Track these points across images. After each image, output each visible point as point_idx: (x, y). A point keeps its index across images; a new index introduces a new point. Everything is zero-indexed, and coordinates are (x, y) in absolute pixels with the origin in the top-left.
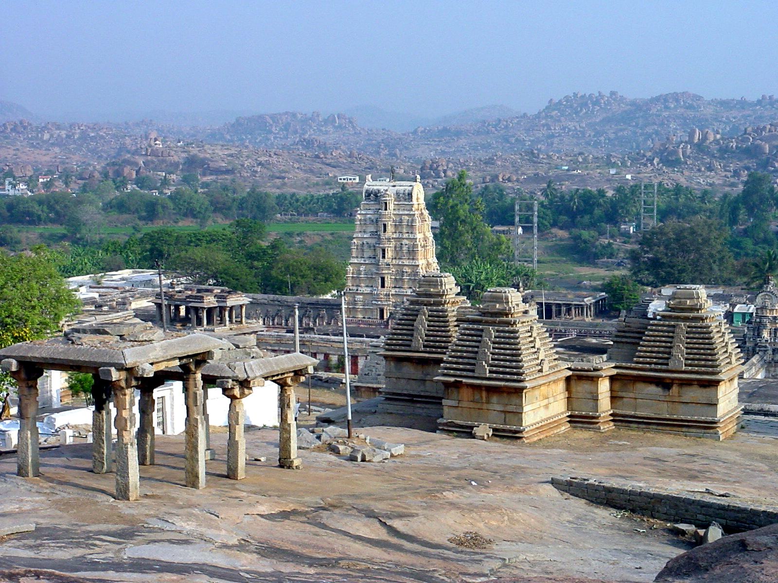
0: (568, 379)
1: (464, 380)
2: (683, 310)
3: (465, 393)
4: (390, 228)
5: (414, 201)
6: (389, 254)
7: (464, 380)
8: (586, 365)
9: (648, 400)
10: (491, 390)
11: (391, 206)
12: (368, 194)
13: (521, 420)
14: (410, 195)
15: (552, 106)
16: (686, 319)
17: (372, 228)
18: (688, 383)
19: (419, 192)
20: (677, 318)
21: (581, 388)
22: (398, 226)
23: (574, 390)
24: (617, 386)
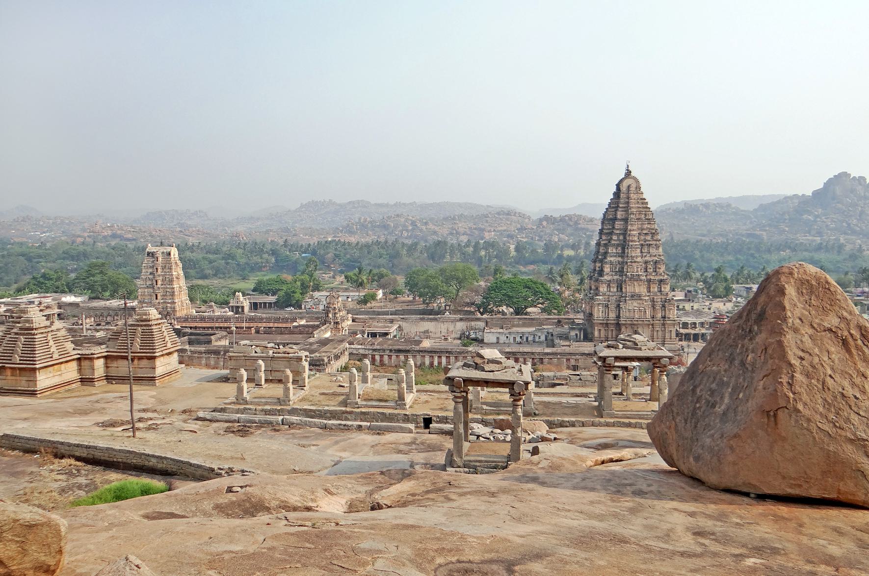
0: (79, 359)
1: (7, 365)
2: (142, 321)
3: (9, 372)
4: (159, 270)
5: (172, 256)
6: (159, 283)
7: (7, 365)
8: (87, 352)
9: (121, 368)
10: (20, 369)
11: (160, 259)
12: (148, 254)
13: (36, 385)
14: (169, 254)
15: (302, 206)
16: (141, 326)
17: (151, 270)
18: (140, 358)
19: (174, 252)
20: (138, 325)
21: (85, 363)
22: (163, 268)
23: (83, 364)
24: (109, 361)
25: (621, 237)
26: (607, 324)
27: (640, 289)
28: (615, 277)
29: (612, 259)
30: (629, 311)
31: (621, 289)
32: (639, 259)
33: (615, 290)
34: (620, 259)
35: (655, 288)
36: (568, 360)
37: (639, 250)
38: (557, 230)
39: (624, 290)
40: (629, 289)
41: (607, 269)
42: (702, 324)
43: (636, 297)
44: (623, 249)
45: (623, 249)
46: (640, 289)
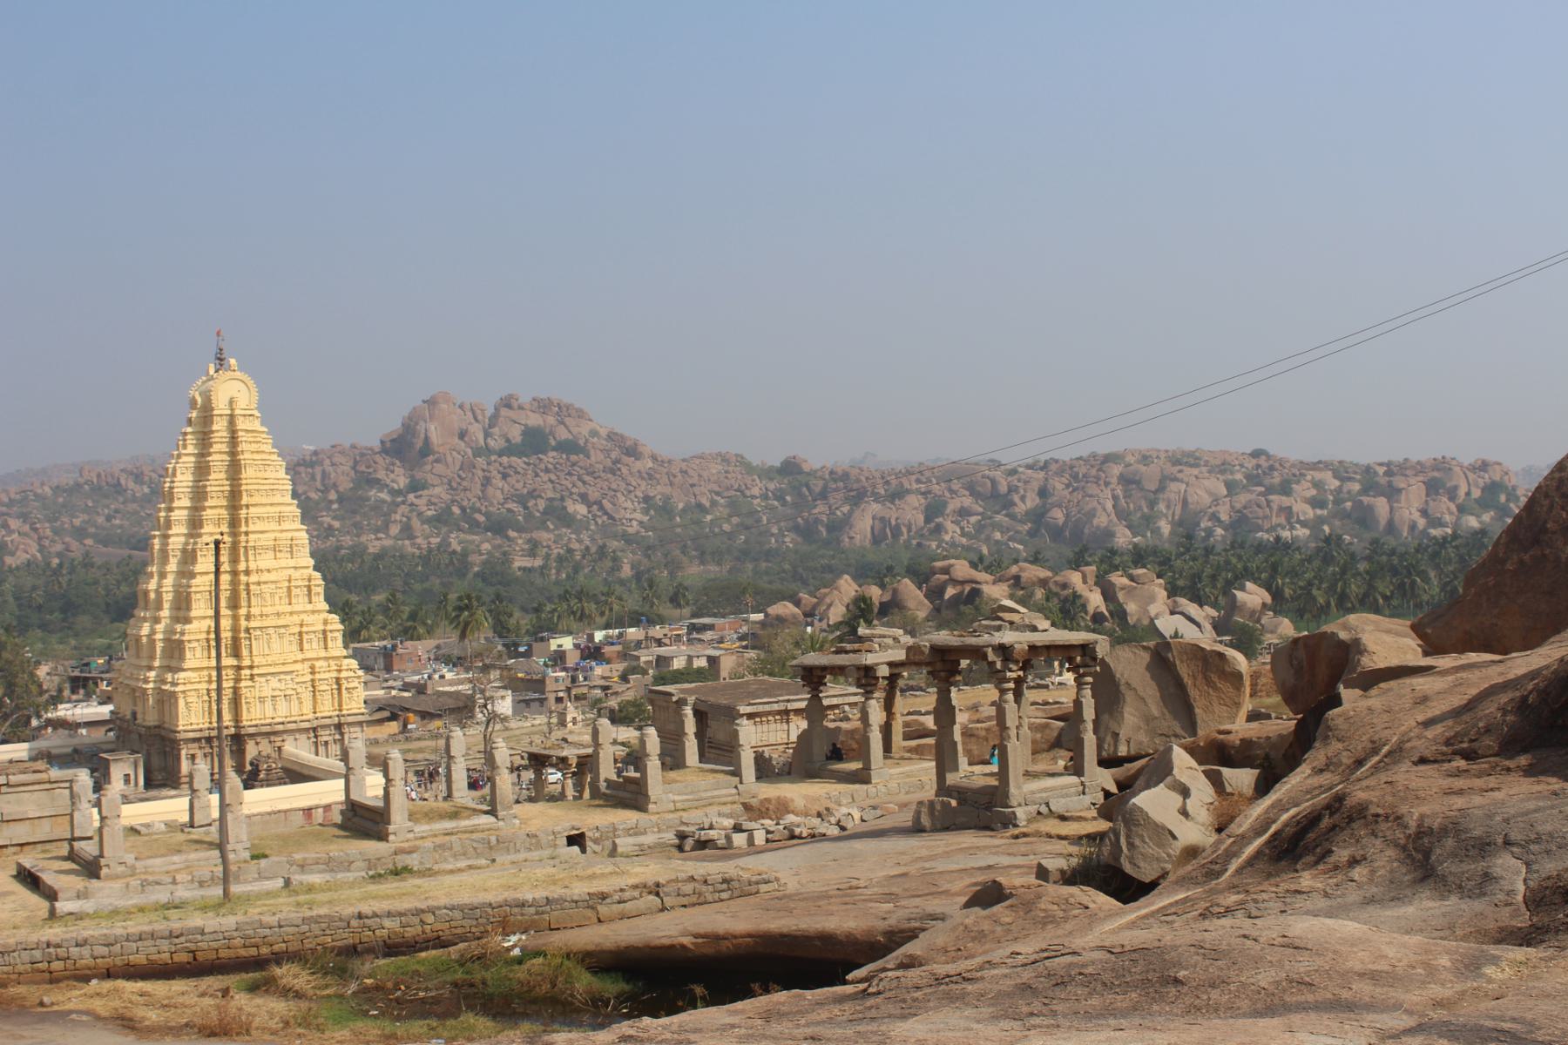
30: (262, 700)
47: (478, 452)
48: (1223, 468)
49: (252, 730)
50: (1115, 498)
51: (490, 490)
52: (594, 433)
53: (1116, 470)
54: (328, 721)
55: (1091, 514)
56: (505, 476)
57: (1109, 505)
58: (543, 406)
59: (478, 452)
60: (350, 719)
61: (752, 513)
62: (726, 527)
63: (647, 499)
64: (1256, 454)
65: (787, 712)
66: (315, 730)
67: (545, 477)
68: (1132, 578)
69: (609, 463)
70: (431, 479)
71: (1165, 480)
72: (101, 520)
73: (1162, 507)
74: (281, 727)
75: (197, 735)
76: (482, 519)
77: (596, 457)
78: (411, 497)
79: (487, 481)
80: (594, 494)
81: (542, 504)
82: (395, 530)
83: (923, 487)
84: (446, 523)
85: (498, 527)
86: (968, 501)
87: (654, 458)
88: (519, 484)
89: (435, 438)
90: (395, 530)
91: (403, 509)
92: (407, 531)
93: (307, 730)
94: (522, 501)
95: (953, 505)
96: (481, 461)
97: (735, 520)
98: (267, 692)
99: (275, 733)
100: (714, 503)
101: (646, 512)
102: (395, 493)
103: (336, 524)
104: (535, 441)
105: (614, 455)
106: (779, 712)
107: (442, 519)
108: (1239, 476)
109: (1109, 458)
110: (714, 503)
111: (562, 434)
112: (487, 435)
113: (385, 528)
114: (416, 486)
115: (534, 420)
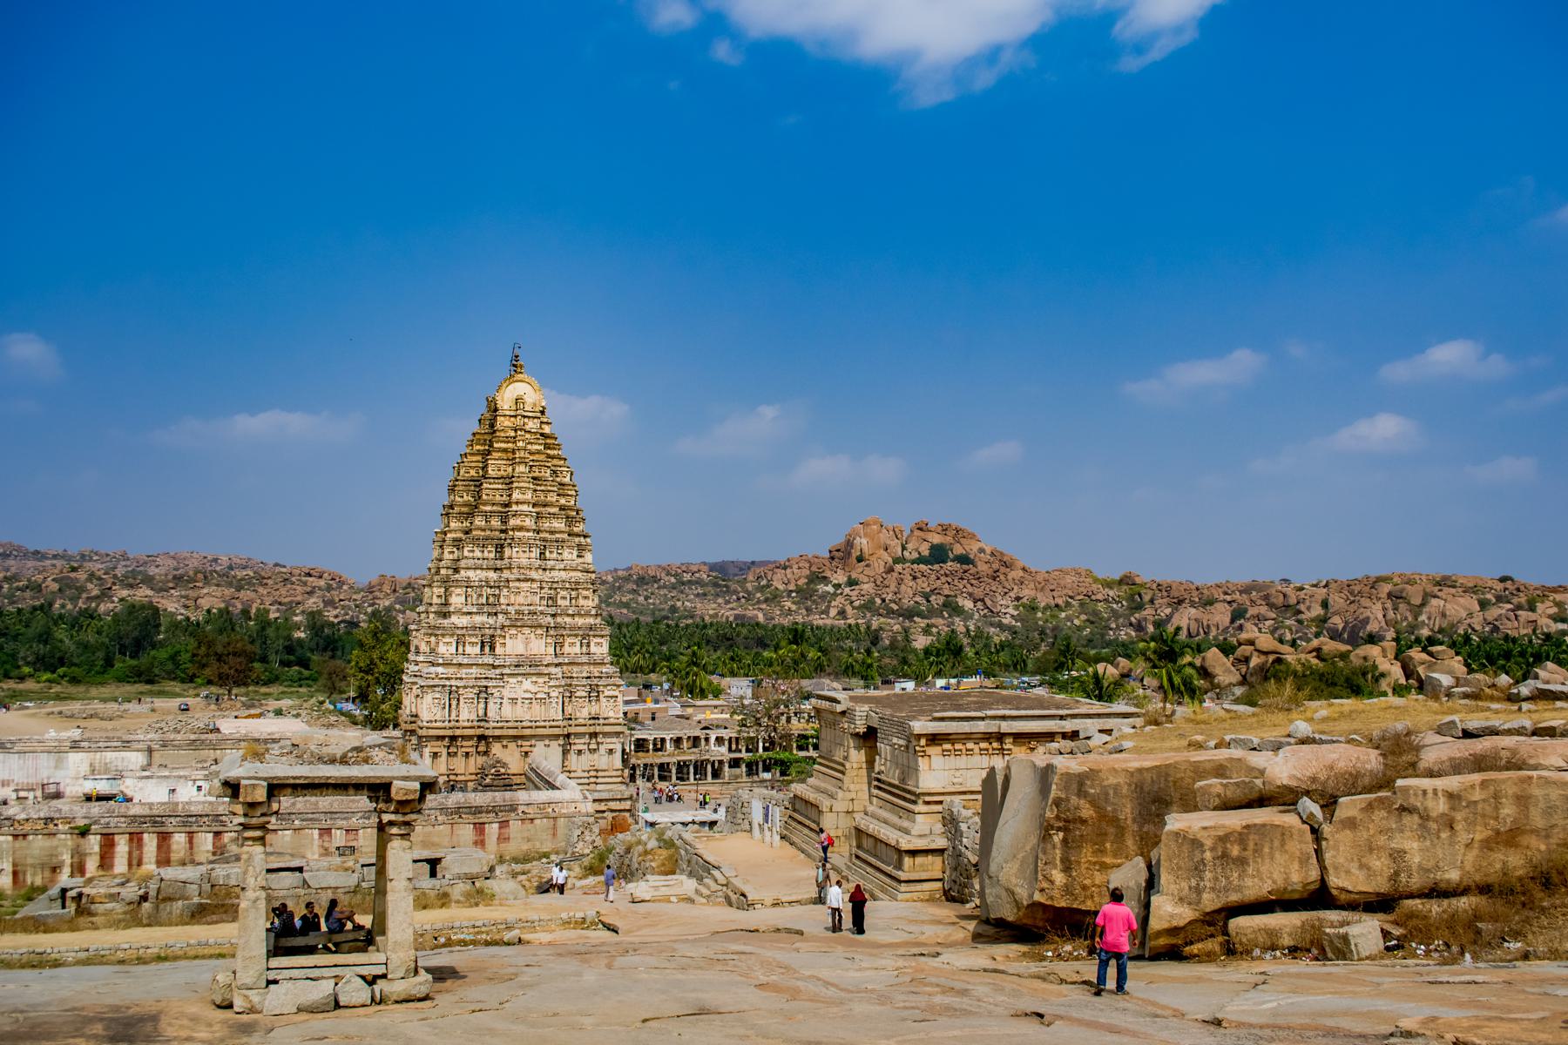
25: (496, 523)
26: (453, 738)
27: (539, 646)
28: (478, 619)
29: (471, 574)
31: (492, 648)
32: (534, 575)
33: (477, 649)
34: (492, 575)
35: (573, 648)
36: (325, 832)
37: (535, 552)
38: (401, 603)
39: (499, 650)
40: (513, 646)
41: (457, 600)
42: (678, 741)
43: (528, 666)
44: (500, 548)
45: (500, 548)
46: (539, 646)
47: (897, 561)
48: (1472, 590)
49: (498, 732)
50: (1384, 609)
51: (903, 587)
52: (982, 550)
53: (1386, 588)
54: (582, 729)
55: (1366, 621)
56: (915, 578)
57: (1380, 616)
58: (945, 529)
59: (897, 561)
60: (607, 729)
61: (1096, 613)
62: (1077, 622)
63: (1018, 599)
64: (1503, 580)
65: (1000, 737)
66: (568, 736)
67: (943, 579)
68: (1431, 654)
69: (990, 572)
70: (863, 578)
71: (1427, 597)
72: (641, 599)
73: (1423, 618)
74: (527, 732)
75: (441, 733)
76: (895, 607)
77: (983, 568)
78: (847, 590)
79: (900, 582)
80: (978, 593)
81: (941, 600)
82: (833, 612)
83: (1228, 598)
84: (869, 609)
85: (909, 614)
86: (1264, 610)
87: (1024, 569)
88: (923, 584)
89: (866, 550)
90: (833, 612)
91: (839, 599)
92: (842, 613)
93: (557, 737)
94: (927, 597)
95: (1252, 611)
96: (898, 567)
97: (1083, 617)
98: (520, 694)
99: (522, 737)
100: (1068, 604)
101: (1016, 608)
102: (837, 586)
103: (794, 607)
104: (938, 555)
105: (996, 566)
106: (987, 737)
107: (868, 606)
108: (1489, 596)
109: (1379, 580)
110: (1068, 604)
111: (958, 550)
112: (904, 548)
113: (826, 612)
114: (852, 583)
115: (936, 539)
